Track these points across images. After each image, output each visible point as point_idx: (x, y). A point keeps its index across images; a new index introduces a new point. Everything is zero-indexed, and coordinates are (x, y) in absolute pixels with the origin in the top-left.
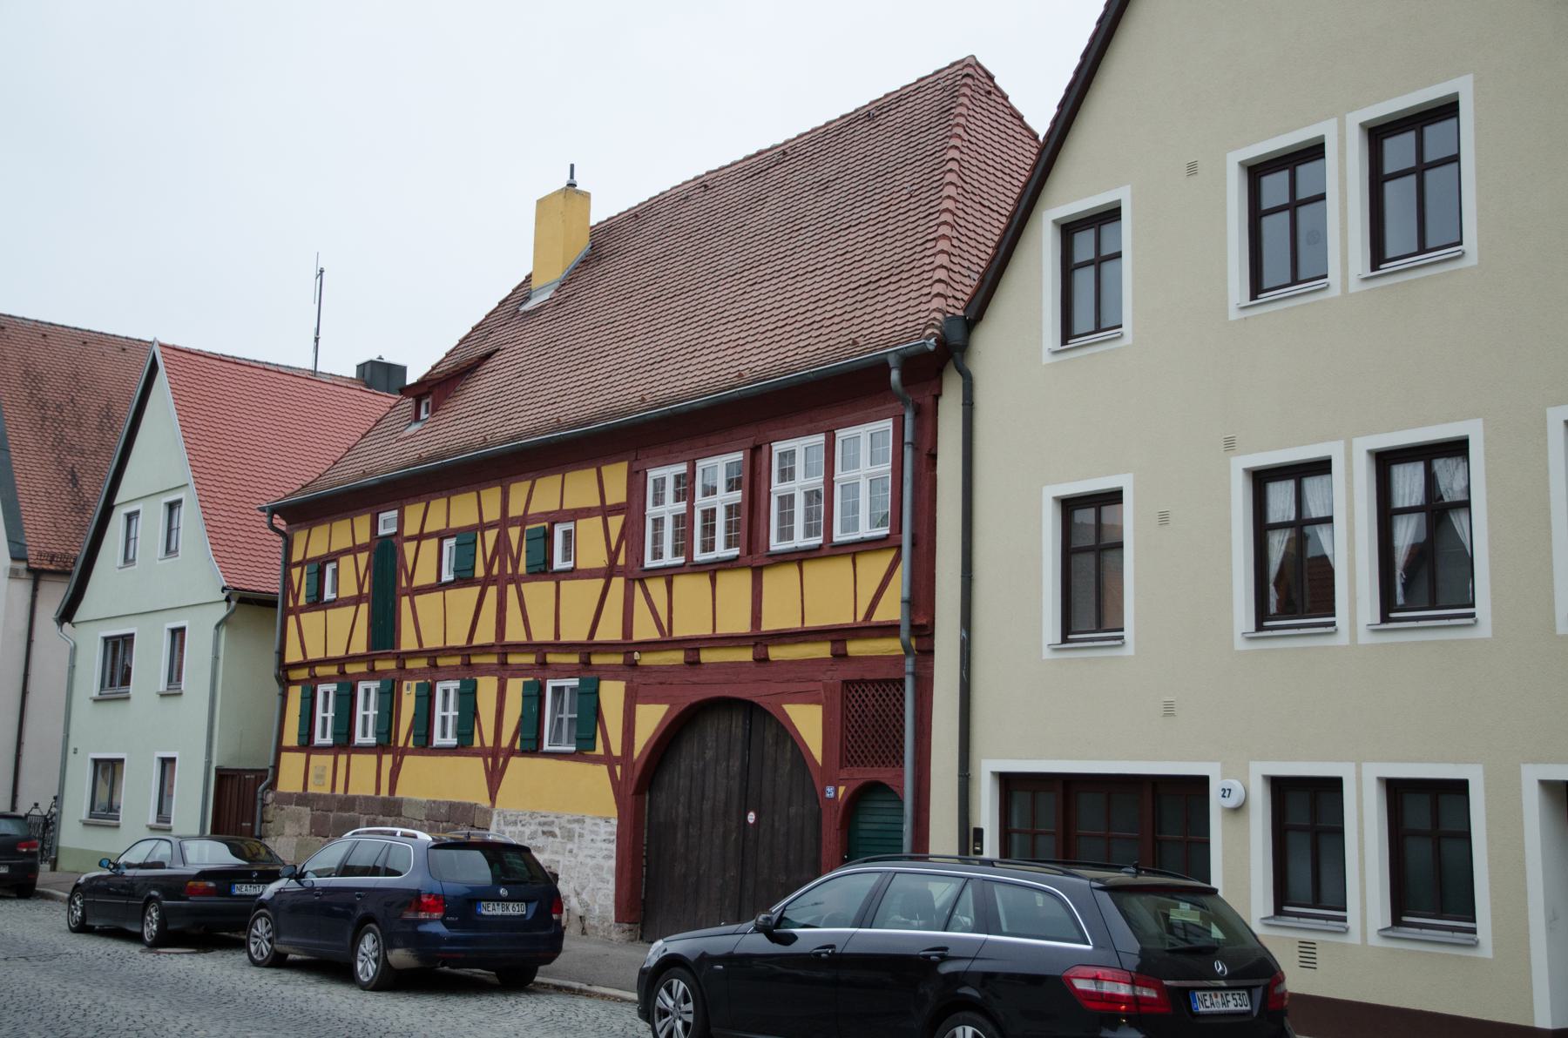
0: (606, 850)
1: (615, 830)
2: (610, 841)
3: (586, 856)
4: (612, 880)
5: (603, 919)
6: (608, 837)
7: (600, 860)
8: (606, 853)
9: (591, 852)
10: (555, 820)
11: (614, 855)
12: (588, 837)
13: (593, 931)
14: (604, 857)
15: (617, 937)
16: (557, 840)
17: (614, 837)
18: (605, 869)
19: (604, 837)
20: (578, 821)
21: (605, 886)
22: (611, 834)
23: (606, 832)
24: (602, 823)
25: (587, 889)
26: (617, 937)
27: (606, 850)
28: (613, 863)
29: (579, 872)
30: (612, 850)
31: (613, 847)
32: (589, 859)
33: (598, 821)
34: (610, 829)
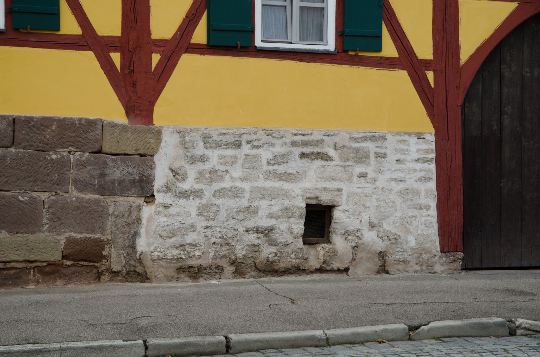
0: (421, 170)
1: (433, 147)
2: (425, 161)
3: (390, 180)
4: (433, 204)
5: (419, 251)
6: (422, 156)
7: (411, 183)
8: (423, 174)
9: (399, 175)
10: (326, 138)
11: (434, 177)
12: (392, 157)
13: (401, 267)
14: (420, 180)
15: (443, 268)
16: (333, 163)
17: (433, 155)
18: (423, 193)
19: (416, 156)
20: (373, 138)
21: (424, 212)
22: (427, 151)
23: (418, 151)
24: (413, 140)
25: (392, 218)
26: (443, 268)
27: (421, 170)
28: (432, 185)
29: (378, 200)
30: (429, 171)
31: (432, 167)
32: (393, 183)
33: (406, 138)
34: (424, 146)
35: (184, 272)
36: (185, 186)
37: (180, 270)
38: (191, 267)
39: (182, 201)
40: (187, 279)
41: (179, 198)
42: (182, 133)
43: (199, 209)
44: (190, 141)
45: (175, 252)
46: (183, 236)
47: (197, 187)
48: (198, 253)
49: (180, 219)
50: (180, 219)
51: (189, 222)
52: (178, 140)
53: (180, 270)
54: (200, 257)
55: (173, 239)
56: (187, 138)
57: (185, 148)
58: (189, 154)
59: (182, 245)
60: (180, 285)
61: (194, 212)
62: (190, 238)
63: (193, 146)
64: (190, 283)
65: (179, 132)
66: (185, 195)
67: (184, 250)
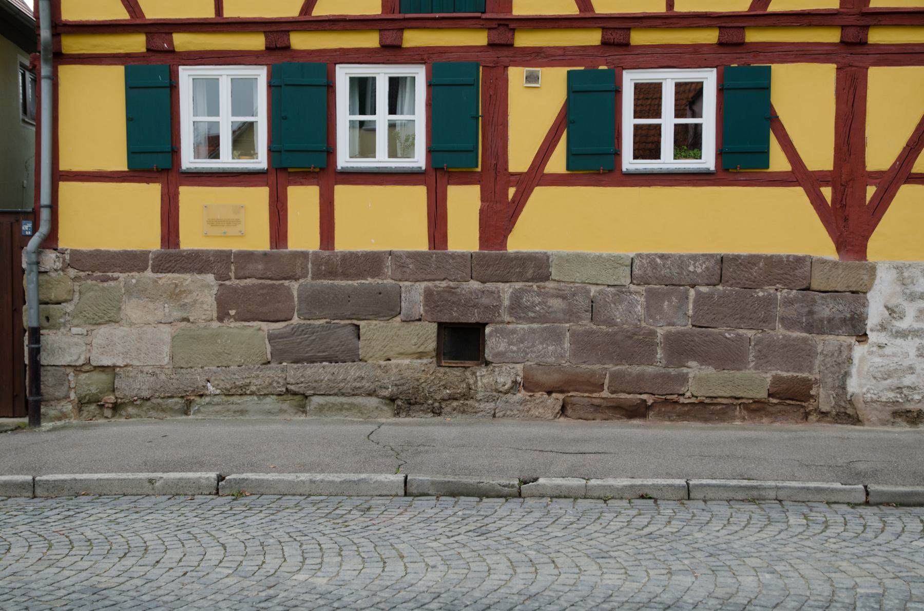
35: (900, 416)
36: (903, 325)
37: (896, 414)
38: (909, 411)
39: (899, 341)
40: (904, 424)
41: (896, 337)
42: (899, 269)
43: (918, 349)
44: (909, 277)
45: (891, 395)
46: (900, 378)
47: (916, 326)
48: (917, 397)
49: (896, 359)
50: (896, 359)
51: (906, 363)
52: (895, 276)
53: (896, 414)
54: (920, 401)
55: (889, 381)
56: (906, 274)
57: (903, 284)
58: (908, 291)
59: (898, 388)
60: (898, 429)
61: (913, 353)
62: (908, 380)
63: (912, 282)
64: (908, 429)
65: (897, 268)
66: (903, 334)
67: (901, 393)
